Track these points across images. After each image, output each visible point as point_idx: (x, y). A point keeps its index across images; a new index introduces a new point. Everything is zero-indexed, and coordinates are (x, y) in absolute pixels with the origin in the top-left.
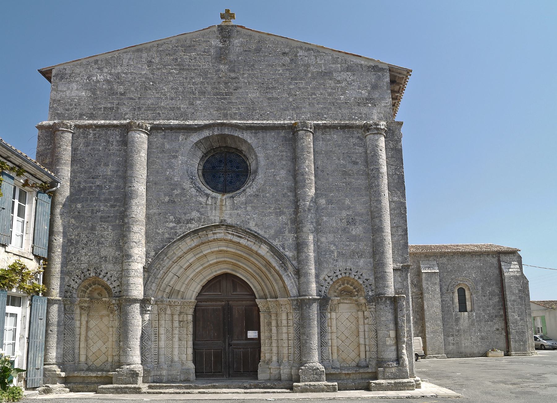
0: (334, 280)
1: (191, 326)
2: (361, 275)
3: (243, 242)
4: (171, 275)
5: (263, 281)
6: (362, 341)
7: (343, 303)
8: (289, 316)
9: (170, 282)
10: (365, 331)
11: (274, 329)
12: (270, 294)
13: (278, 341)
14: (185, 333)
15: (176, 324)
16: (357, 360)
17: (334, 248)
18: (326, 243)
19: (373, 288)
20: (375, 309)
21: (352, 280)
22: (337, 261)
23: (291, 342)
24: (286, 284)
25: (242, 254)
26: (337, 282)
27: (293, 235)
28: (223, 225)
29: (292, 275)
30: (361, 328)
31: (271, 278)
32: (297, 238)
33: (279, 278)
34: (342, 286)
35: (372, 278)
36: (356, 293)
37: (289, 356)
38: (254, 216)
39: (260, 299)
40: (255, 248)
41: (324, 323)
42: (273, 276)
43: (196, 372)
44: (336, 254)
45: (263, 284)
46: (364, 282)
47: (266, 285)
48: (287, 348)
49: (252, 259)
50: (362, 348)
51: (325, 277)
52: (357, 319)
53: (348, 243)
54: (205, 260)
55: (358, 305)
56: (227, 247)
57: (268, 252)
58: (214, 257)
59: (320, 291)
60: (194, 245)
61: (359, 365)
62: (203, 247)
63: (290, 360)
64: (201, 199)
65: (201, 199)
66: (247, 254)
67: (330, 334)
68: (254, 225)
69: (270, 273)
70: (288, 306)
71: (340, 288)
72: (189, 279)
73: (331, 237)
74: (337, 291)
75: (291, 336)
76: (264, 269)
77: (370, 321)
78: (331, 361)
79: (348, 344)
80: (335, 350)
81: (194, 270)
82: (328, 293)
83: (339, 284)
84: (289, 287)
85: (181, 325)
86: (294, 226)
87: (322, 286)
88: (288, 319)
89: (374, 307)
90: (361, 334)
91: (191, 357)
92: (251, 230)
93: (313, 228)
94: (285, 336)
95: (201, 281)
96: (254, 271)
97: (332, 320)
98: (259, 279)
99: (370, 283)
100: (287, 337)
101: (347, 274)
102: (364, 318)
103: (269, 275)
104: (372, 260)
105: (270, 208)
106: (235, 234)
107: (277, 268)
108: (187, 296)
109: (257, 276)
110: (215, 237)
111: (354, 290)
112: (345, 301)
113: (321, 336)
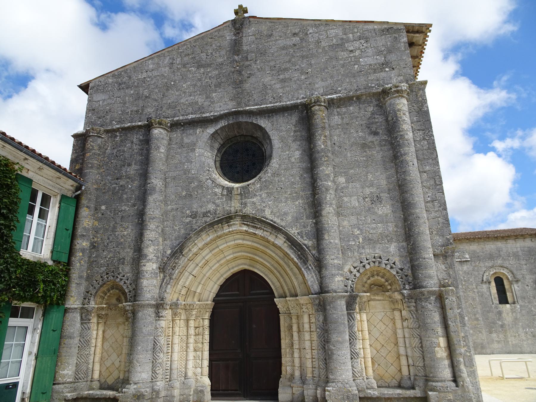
0: (361, 271)
1: (207, 332)
2: (394, 263)
3: (259, 232)
4: (187, 274)
5: (283, 277)
6: (402, 351)
7: (374, 300)
8: (311, 319)
9: (185, 283)
10: (404, 337)
11: (295, 334)
12: (290, 292)
13: (300, 351)
14: (201, 341)
15: (192, 331)
16: (398, 377)
17: (358, 232)
18: (348, 227)
19: (411, 279)
20: (416, 307)
21: (382, 271)
23: (315, 352)
24: (307, 278)
25: (259, 246)
26: (365, 273)
27: (311, 220)
28: (238, 216)
29: (312, 268)
30: (400, 332)
31: (289, 272)
32: (316, 224)
33: (298, 272)
34: (372, 279)
35: (407, 266)
36: (389, 287)
37: (313, 371)
38: (269, 203)
39: (279, 298)
40: (271, 238)
41: (353, 327)
42: (291, 269)
43: (211, 390)
44: (361, 240)
45: (282, 280)
46: (397, 273)
47: (285, 280)
48: (310, 360)
49: (269, 251)
50: (404, 361)
51: (350, 269)
52: (393, 320)
53: (374, 226)
54: (222, 256)
55: (393, 302)
56: (243, 239)
57: (285, 242)
58: (231, 251)
59: (346, 286)
60: (209, 239)
61: (402, 385)
62: (219, 242)
63: (315, 377)
64: (217, 190)
65: (217, 190)
66: (264, 246)
67: (361, 341)
68: (270, 213)
69: (289, 266)
70: (309, 306)
71: (369, 281)
72: (205, 278)
73: (353, 220)
74: (366, 285)
75: (315, 344)
76: (281, 262)
77: (411, 323)
78: (365, 380)
79: (384, 355)
80: (370, 364)
81: (211, 268)
82: (356, 288)
83: (367, 277)
84: (309, 282)
85: (197, 333)
86: (312, 211)
87: (348, 279)
88: (310, 323)
89: (414, 304)
90: (401, 341)
91: (206, 370)
92: (267, 219)
93: (333, 211)
94: (307, 344)
95: (218, 279)
96: (272, 265)
97: (362, 322)
98: (278, 274)
99: (406, 274)
100: (310, 345)
101: (377, 264)
102: (402, 319)
103: (288, 269)
104: (404, 244)
105: (286, 192)
106: (250, 224)
107: (295, 259)
108: (204, 298)
109: (275, 271)
110: (231, 230)
111: (387, 283)
112: (377, 298)
113: (350, 344)
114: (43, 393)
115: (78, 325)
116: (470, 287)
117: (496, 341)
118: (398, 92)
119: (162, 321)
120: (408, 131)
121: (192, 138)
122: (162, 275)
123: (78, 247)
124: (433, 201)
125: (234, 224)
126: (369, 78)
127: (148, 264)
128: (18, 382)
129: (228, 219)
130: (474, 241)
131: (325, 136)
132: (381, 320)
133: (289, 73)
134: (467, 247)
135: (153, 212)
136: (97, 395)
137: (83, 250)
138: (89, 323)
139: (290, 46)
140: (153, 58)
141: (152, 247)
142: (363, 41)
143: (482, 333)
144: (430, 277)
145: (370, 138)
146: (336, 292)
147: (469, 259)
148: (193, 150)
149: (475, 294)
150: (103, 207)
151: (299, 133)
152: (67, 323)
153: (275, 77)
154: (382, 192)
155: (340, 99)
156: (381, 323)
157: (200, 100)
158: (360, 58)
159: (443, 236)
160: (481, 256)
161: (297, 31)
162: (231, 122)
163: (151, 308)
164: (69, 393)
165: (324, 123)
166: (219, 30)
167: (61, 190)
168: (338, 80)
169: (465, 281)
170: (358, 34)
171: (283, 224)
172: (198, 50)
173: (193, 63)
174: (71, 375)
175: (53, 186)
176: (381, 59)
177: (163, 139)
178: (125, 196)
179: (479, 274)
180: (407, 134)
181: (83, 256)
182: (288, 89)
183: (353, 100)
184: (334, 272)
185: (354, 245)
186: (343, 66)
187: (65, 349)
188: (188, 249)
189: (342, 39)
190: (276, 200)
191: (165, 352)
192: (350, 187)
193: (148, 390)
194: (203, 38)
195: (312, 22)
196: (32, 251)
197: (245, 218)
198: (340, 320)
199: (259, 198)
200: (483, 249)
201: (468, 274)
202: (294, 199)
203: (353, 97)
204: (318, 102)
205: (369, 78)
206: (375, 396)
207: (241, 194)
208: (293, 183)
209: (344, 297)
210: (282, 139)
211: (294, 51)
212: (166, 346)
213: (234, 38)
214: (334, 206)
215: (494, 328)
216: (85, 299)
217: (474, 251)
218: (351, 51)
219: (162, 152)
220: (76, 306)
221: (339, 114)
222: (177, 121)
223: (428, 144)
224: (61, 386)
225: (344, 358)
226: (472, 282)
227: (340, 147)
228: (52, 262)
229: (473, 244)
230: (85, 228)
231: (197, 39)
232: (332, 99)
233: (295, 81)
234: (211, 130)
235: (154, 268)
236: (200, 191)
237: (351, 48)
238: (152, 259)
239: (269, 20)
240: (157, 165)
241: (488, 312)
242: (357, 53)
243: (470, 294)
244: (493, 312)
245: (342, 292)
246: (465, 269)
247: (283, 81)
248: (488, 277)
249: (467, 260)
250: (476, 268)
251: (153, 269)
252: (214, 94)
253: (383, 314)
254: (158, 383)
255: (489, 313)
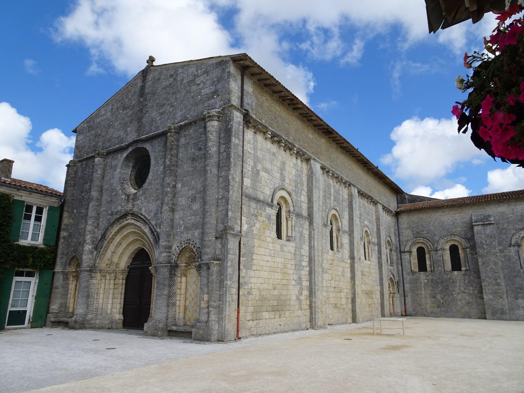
2: (196, 244)
3: (138, 224)
22: (183, 233)
46: (197, 250)
53: (190, 218)
114: (40, 317)
115: (61, 281)
116: (492, 251)
117: (522, 307)
118: (209, 117)
119: (93, 280)
120: (212, 147)
121: (116, 161)
122: (96, 252)
123: (61, 236)
124: (222, 198)
125: (128, 219)
126: (205, 105)
127: (86, 246)
128: (27, 310)
129: (125, 216)
130: (503, 202)
131: (171, 155)
132: (194, 282)
133: (165, 108)
134: (494, 209)
135: (91, 213)
136: (65, 320)
137: (64, 238)
138: (67, 280)
139: (168, 86)
140: (104, 106)
141: (90, 235)
142: (205, 75)
143: (503, 298)
144: (207, 254)
145: (197, 153)
146: (161, 263)
147: (493, 222)
148: (115, 170)
149: (497, 259)
150: (75, 211)
151: (164, 153)
152: (55, 280)
153: (158, 112)
154: (197, 193)
155: (186, 125)
156: (194, 284)
157: (122, 133)
158: (202, 89)
159: (223, 225)
160: (511, 217)
161: (172, 73)
162: (134, 148)
163: (87, 272)
164: (54, 318)
165: (172, 145)
166: (136, 79)
167: (47, 203)
168: (188, 109)
169: (487, 245)
170: (204, 69)
171: (149, 218)
172: (124, 96)
173: (122, 107)
174: (57, 309)
175: (42, 202)
176: (213, 88)
177: (100, 164)
178: (84, 203)
179: (507, 237)
180: (211, 149)
181: (64, 241)
182: (163, 120)
183: (192, 124)
184: (162, 250)
185: (179, 231)
186: (193, 97)
187: (54, 294)
188: (107, 236)
189: (195, 75)
190: (148, 202)
191: (95, 298)
192: (183, 190)
193: (81, 319)
194: (127, 87)
195: (181, 63)
196: (32, 240)
197: (133, 214)
198: (161, 281)
199: (140, 201)
200: (513, 210)
201: (491, 237)
202: (156, 200)
203: (192, 122)
204: (170, 130)
205: (205, 105)
206: (174, 330)
207: (133, 199)
208: (157, 190)
209: (168, 266)
210: (156, 159)
211: (169, 90)
212: (96, 295)
213: (142, 84)
214: (170, 205)
215: (521, 294)
216: (65, 266)
217: (503, 213)
218: (198, 84)
219: (99, 174)
220: (59, 271)
221: (185, 136)
222: (110, 150)
223: (227, 154)
224: (51, 314)
225: (160, 305)
226: (495, 246)
227: (182, 161)
228: (44, 246)
229: (502, 205)
230: (65, 224)
231: (125, 88)
232: (181, 125)
233: (167, 113)
234: (125, 155)
235: (90, 248)
236: (116, 198)
237: (198, 82)
238: (89, 243)
239: (159, 67)
240: (95, 183)
241: (515, 277)
242: (202, 85)
243: (493, 258)
244: (521, 277)
245: (166, 264)
246: (487, 233)
247: (161, 114)
248: (517, 240)
249: (490, 222)
250: (504, 231)
251: (89, 249)
252: (128, 129)
253: (196, 278)
254: (89, 316)
255: (516, 278)
